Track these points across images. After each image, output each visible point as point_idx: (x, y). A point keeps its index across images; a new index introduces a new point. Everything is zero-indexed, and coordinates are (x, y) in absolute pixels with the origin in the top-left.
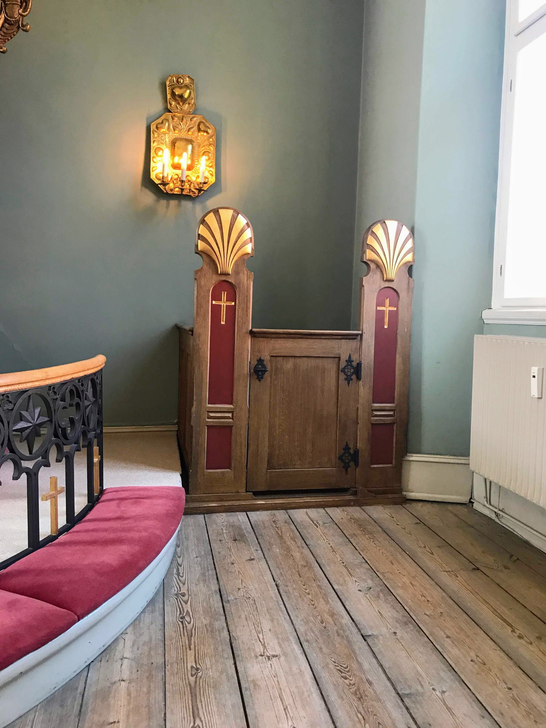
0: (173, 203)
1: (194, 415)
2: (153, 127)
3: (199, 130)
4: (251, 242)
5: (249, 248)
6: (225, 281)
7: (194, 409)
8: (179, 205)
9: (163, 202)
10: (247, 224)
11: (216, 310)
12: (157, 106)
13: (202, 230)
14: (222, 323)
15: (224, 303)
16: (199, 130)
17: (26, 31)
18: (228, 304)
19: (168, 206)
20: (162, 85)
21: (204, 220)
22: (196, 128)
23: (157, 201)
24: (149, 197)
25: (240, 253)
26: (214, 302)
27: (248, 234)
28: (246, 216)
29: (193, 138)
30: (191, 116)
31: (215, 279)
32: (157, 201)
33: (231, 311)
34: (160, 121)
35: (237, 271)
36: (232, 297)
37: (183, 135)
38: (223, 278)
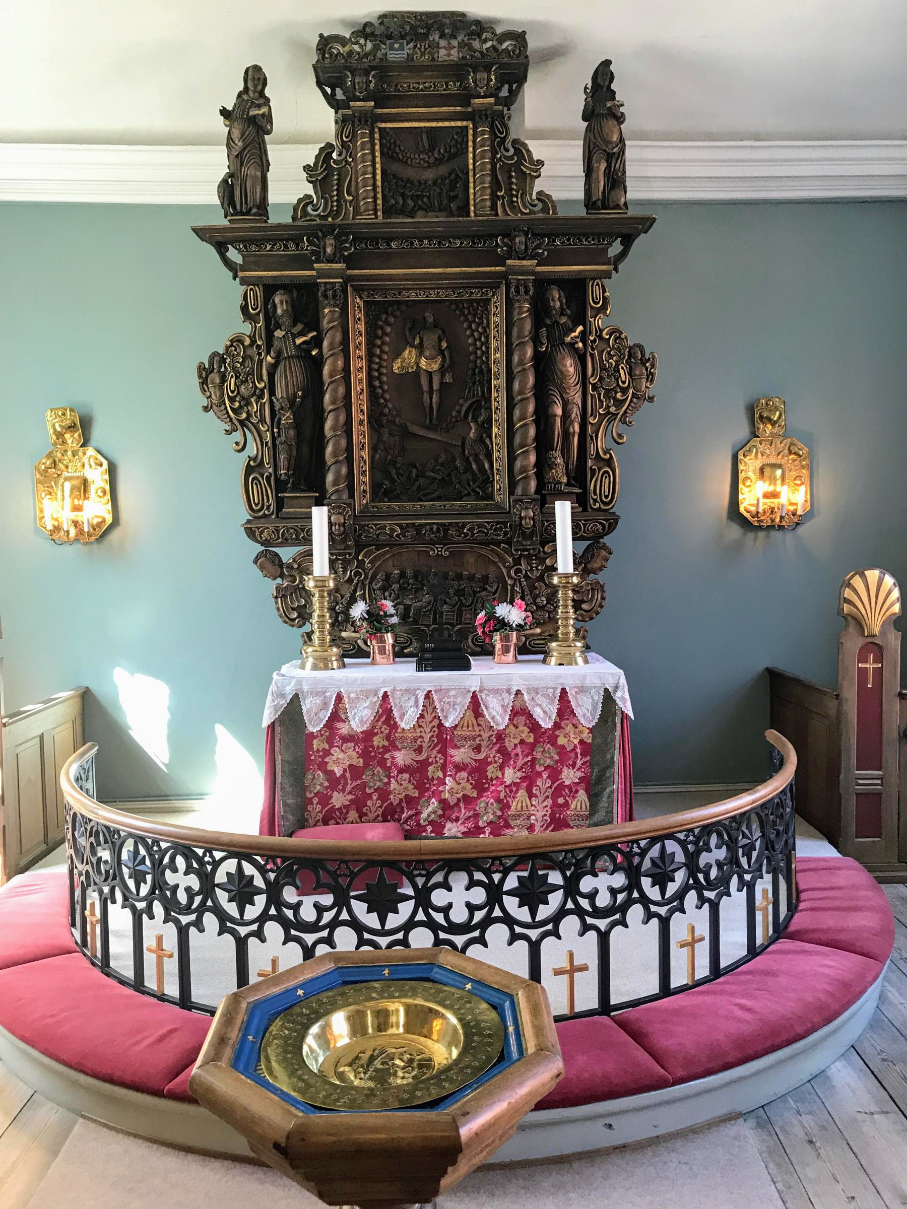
0: (761, 534)
1: (842, 783)
2: (741, 457)
3: (790, 453)
4: (898, 601)
5: (896, 608)
6: (871, 643)
7: (842, 777)
8: (768, 537)
9: (750, 535)
10: (894, 584)
11: (863, 672)
12: (744, 431)
13: (848, 594)
14: (869, 686)
15: (871, 666)
16: (790, 453)
17: (651, 399)
18: (875, 666)
19: (755, 539)
20: (747, 409)
21: (850, 583)
22: (786, 452)
23: (745, 534)
24: (735, 531)
25: (888, 614)
26: (860, 665)
27: (896, 593)
28: (893, 575)
29: (783, 462)
30: (781, 439)
31: (860, 642)
32: (745, 534)
33: (879, 673)
34: (747, 448)
35: (883, 632)
36: (879, 659)
37: (772, 460)
38: (870, 640)
